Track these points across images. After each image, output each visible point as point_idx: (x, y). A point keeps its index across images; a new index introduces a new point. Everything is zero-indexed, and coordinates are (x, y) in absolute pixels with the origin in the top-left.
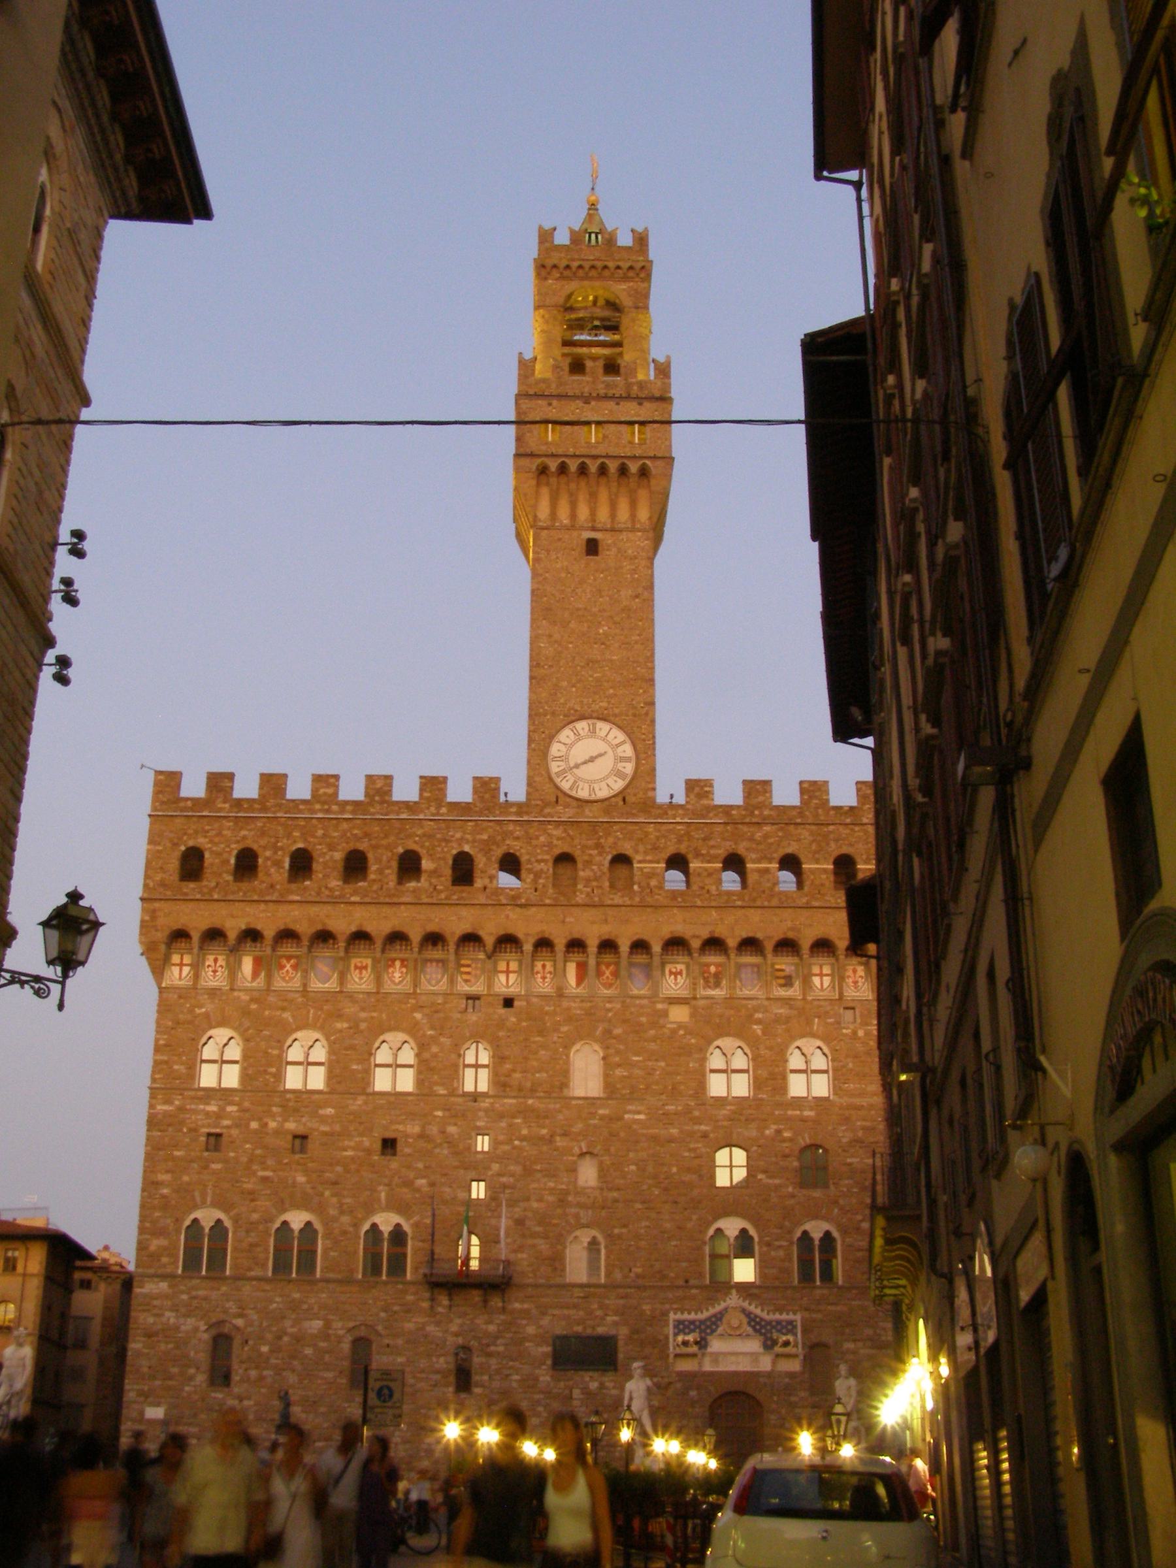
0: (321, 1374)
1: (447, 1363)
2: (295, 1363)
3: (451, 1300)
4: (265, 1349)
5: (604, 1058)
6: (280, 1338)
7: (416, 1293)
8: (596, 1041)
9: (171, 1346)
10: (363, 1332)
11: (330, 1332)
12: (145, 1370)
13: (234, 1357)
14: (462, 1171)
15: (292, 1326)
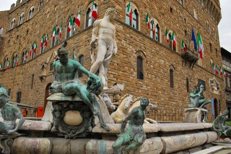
0: (165, 80)
1: (186, 82)
2: (159, 74)
3: (186, 63)
4: (152, 66)
5: (197, 13)
6: (155, 63)
7: (179, 59)
8: (196, 8)
9: (125, 56)
10: (172, 68)
11: (166, 65)
12: (116, 65)
13: (144, 68)
14: (183, 27)
15: (158, 60)
